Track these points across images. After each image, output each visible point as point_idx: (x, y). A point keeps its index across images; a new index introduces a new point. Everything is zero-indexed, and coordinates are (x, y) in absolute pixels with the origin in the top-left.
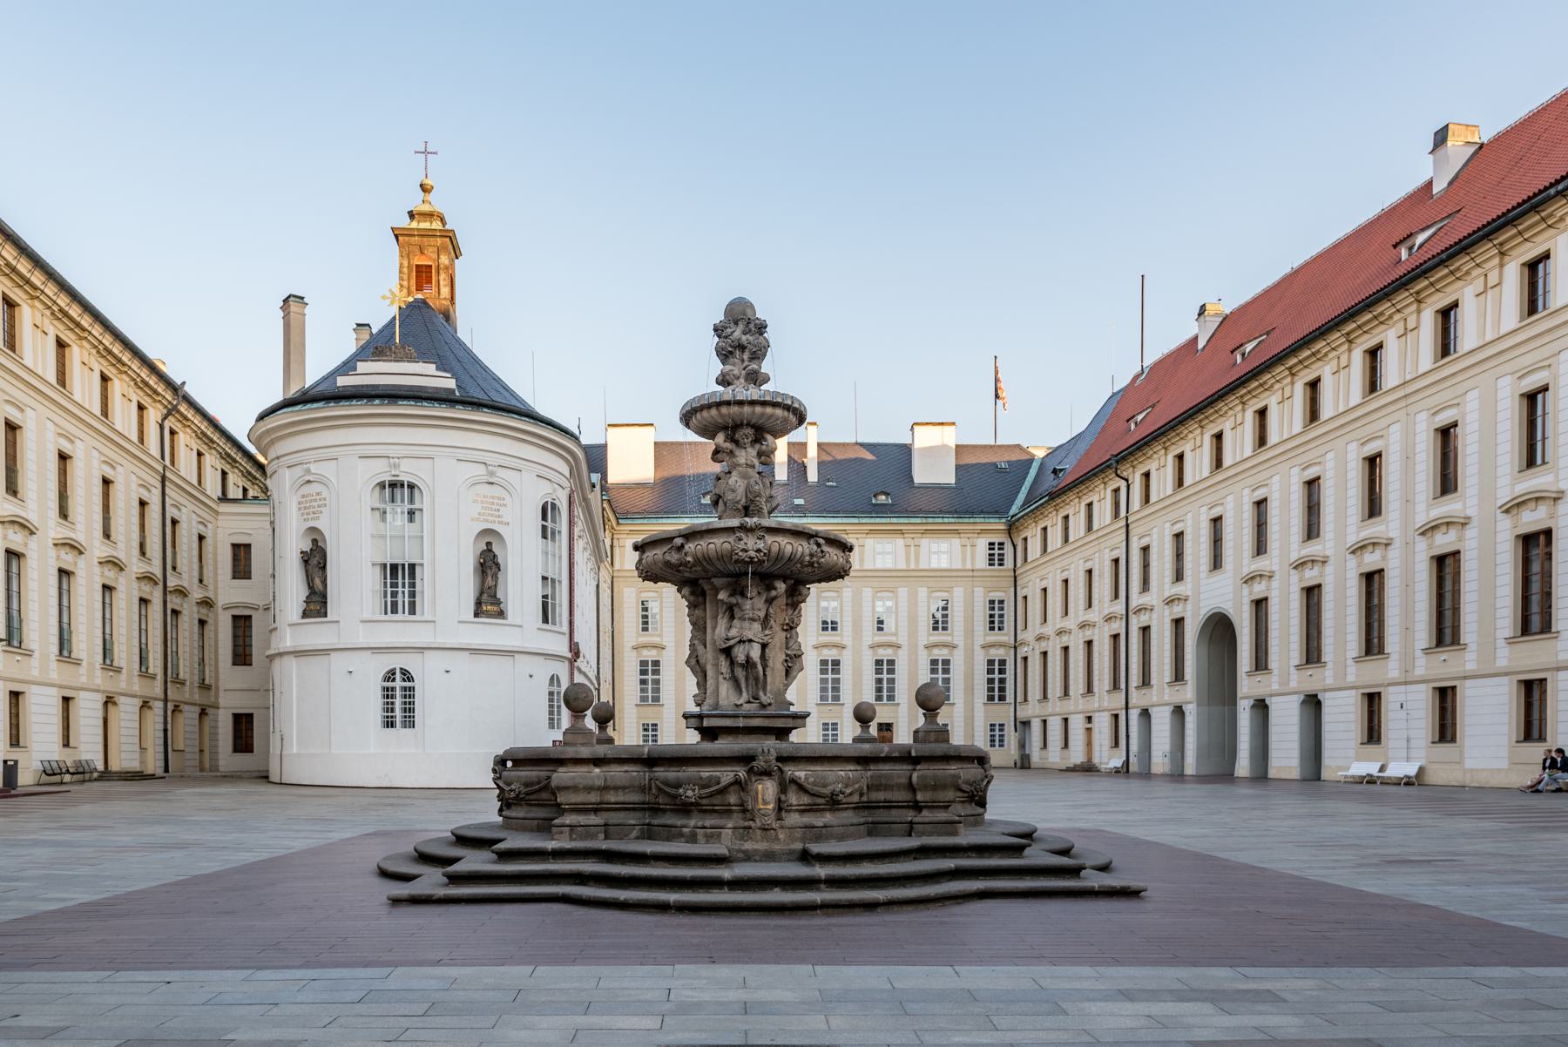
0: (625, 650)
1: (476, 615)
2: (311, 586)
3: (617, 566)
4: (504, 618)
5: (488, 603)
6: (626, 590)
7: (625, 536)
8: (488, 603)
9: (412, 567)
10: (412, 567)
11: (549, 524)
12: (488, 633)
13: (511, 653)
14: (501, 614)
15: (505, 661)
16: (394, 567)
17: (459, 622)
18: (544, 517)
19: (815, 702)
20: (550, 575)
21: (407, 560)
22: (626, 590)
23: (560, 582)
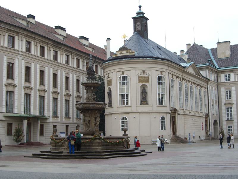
0: (222, 105)
1: (141, 104)
2: (109, 100)
3: (219, 82)
4: (148, 104)
5: (144, 100)
6: (222, 88)
7: (220, 73)
8: (144, 100)
9: (127, 95)
10: (127, 95)
11: (160, 81)
12: (145, 108)
13: (149, 113)
14: (147, 104)
15: (148, 115)
16: (124, 95)
17: (137, 106)
18: (159, 80)
19: (225, 120)
20: (161, 93)
21: (125, 93)
22: (222, 88)
23: (164, 94)
